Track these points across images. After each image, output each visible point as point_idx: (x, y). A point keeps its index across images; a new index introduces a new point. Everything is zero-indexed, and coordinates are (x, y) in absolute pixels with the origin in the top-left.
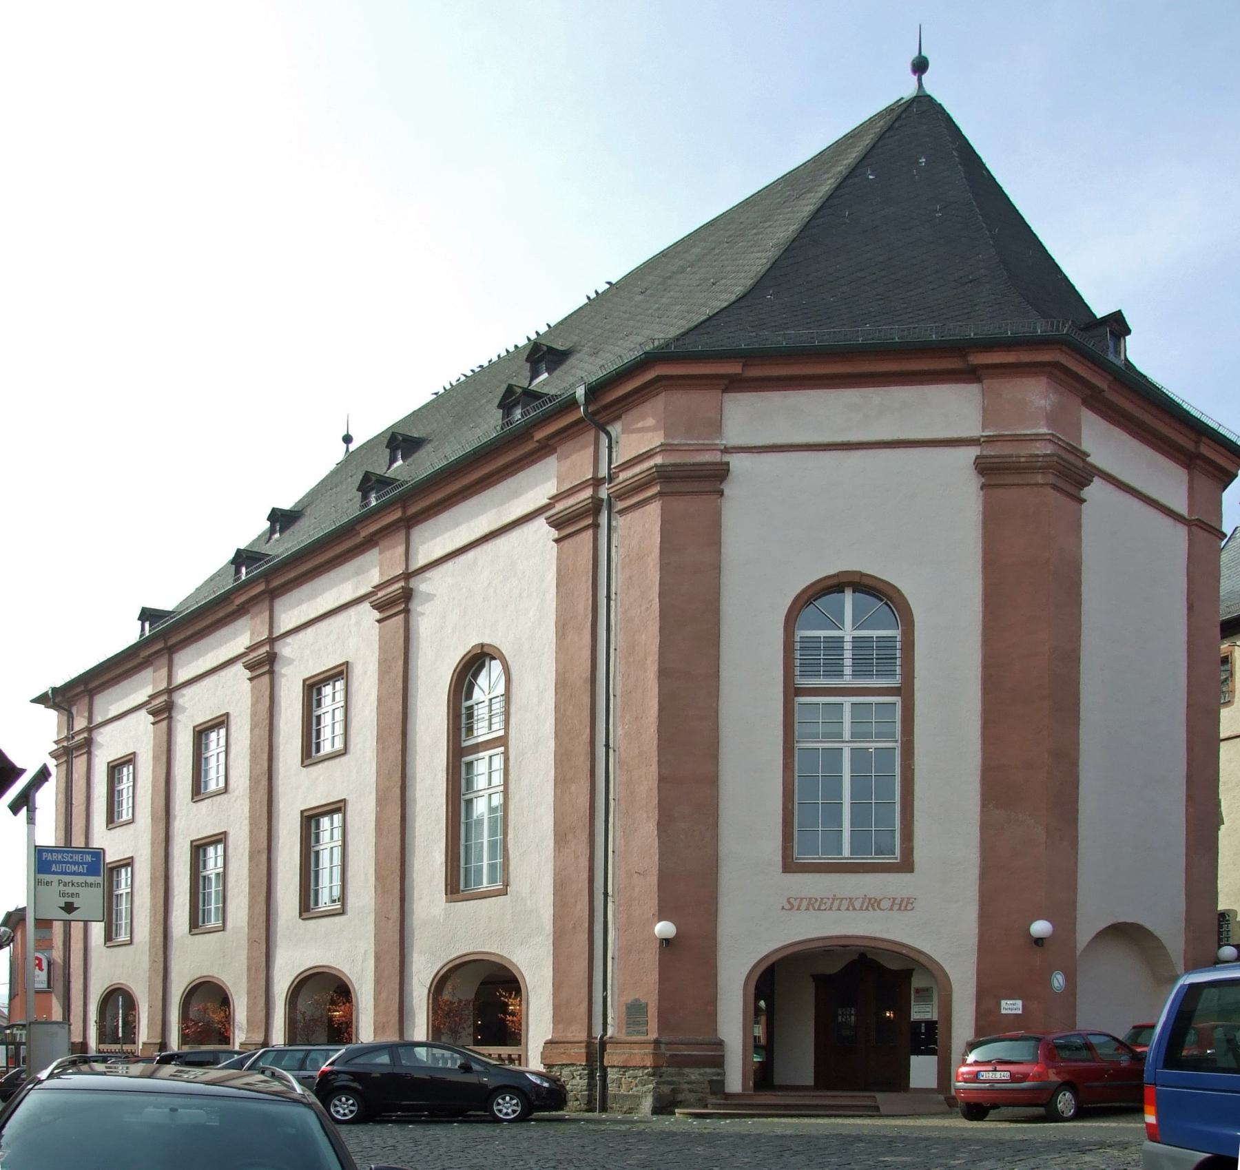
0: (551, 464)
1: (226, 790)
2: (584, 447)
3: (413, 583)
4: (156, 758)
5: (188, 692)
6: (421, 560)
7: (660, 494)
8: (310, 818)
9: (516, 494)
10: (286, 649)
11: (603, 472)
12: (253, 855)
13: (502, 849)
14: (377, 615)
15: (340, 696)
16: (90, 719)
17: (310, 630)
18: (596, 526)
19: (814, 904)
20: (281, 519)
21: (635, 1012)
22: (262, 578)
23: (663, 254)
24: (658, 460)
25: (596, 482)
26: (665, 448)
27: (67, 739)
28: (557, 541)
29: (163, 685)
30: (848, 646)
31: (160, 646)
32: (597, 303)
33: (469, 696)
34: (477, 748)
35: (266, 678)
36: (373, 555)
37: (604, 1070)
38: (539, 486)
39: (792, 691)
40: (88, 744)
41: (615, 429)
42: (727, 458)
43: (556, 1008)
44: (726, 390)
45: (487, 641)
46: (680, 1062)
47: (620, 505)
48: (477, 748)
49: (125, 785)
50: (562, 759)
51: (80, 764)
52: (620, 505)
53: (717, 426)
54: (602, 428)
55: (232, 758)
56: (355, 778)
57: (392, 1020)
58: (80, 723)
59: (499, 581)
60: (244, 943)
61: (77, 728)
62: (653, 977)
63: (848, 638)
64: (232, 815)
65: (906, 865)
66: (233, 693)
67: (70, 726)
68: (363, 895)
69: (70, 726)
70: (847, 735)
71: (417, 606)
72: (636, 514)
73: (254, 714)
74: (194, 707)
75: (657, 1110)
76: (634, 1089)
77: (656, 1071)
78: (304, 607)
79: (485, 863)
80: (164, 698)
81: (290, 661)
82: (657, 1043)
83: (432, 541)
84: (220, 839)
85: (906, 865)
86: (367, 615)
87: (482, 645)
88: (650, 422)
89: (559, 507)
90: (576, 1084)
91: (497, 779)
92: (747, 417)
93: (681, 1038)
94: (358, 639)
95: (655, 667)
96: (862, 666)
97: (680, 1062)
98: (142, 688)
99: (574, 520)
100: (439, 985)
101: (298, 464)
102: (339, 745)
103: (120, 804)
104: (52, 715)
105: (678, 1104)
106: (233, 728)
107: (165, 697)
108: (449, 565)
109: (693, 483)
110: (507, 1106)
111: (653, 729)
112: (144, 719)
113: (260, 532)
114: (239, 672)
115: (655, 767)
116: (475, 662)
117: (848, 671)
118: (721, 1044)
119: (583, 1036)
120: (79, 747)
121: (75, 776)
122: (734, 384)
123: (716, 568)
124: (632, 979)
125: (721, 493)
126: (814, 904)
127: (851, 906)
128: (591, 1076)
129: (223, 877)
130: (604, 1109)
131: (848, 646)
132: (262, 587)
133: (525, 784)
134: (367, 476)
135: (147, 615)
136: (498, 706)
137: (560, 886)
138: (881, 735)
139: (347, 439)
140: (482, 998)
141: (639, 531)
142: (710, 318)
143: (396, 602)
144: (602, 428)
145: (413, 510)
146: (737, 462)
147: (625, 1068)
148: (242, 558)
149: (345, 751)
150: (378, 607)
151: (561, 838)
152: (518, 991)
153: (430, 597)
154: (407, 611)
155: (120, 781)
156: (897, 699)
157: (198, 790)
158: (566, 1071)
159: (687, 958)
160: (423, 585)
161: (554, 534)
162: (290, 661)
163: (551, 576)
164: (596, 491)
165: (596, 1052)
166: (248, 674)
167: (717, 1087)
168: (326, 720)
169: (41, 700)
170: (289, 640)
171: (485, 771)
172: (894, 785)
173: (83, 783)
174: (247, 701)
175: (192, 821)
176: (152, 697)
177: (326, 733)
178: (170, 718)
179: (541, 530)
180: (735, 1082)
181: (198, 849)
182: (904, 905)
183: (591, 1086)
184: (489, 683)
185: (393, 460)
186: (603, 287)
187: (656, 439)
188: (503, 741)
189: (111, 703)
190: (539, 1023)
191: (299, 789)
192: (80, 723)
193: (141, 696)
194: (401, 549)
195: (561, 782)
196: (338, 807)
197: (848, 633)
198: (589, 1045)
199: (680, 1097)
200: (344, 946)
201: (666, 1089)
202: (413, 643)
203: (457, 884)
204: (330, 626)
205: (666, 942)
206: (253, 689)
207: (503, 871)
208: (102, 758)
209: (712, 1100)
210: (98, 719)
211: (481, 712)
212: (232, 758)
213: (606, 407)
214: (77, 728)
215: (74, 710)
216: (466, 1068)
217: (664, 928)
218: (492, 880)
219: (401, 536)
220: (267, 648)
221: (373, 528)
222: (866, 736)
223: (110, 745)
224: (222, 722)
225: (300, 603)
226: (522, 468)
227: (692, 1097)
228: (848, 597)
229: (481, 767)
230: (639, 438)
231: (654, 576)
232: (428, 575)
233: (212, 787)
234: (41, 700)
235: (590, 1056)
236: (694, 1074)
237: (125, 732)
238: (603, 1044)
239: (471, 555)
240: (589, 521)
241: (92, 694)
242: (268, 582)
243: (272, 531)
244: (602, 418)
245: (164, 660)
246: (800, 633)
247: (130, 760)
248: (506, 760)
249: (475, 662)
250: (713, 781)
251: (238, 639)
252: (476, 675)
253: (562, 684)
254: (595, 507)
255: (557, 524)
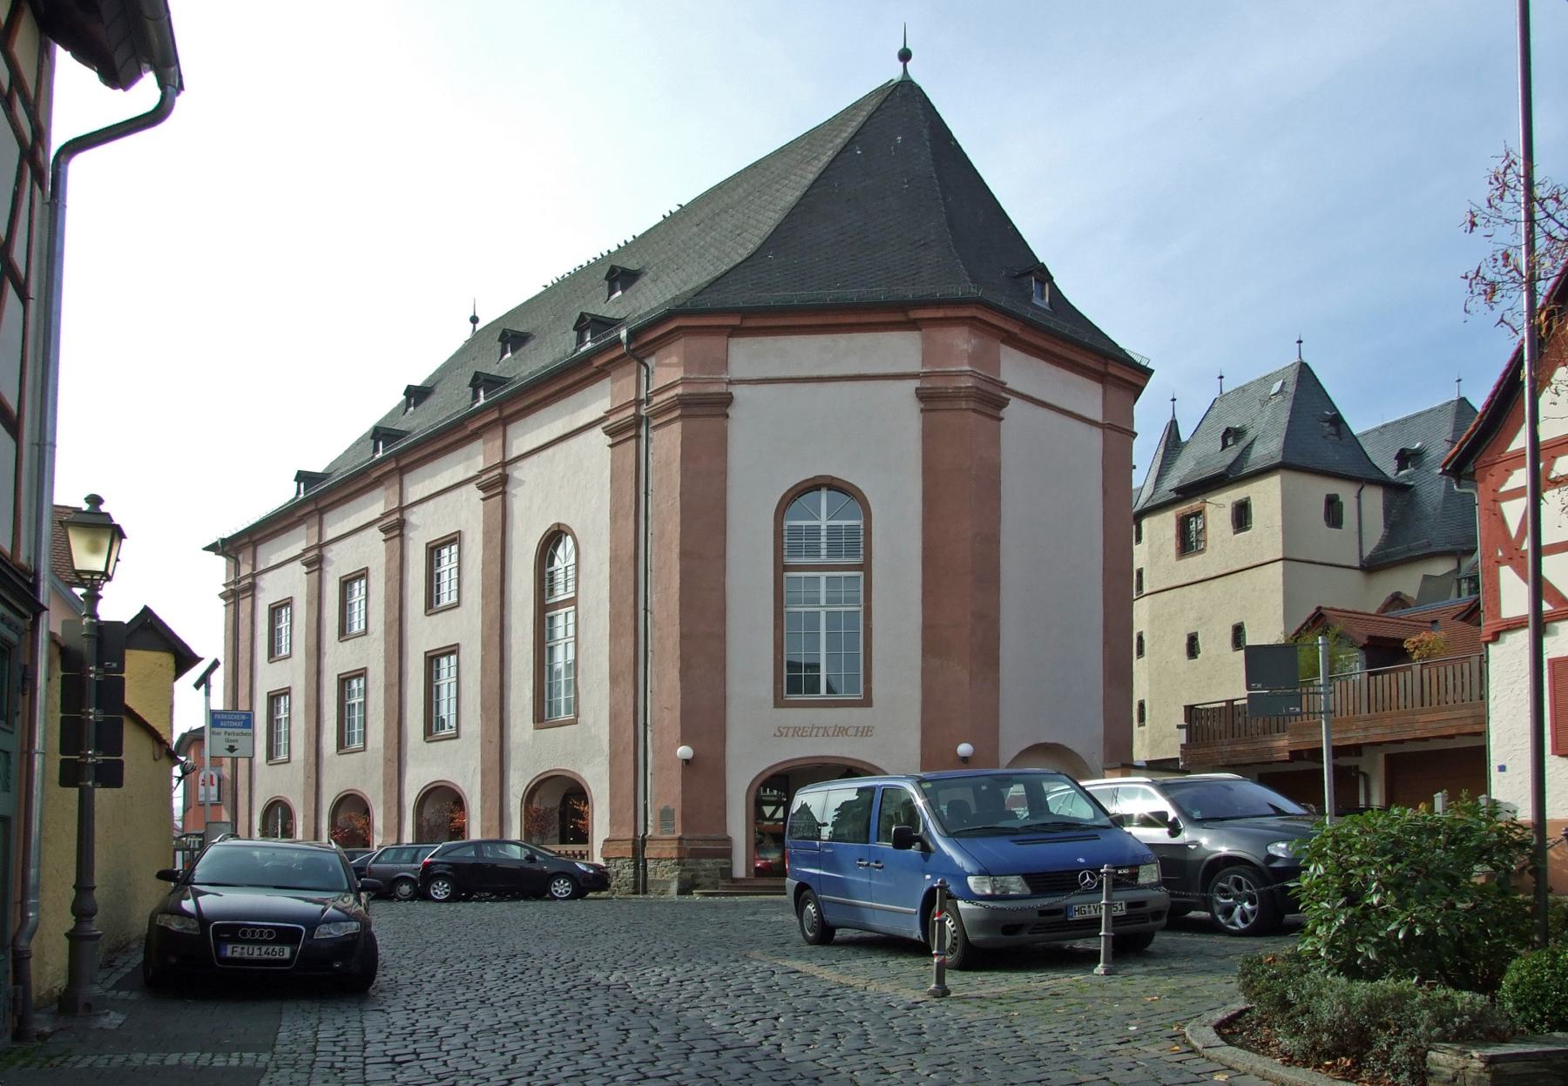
0: (605, 385)
1: (366, 632)
2: (630, 374)
3: (509, 470)
4: (309, 603)
5: (335, 547)
6: (515, 451)
7: (681, 417)
8: (432, 658)
9: (583, 406)
10: (414, 517)
11: (643, 396)
12: (387, 688)
13: (574, 686)
14: (481, 494)
15: (454, 558)
16: (254, 568)
17: (431, 503)
18: (638, 437)
19: (798, 732)
20: (416, 395)
21: (666, 815)
22: (394, 453)
23: (720, 186)
24: (679, 390)
25: (638, 403)
26: (684, 381)
27: (234, 582)
28: (611, 446)
29: (315, 541)
30: (823, 533)
31: (312, 507)
32: (671, 221)
33: (551, 564)
34: (556, 606)
35: (397, 541)
36: (478, 445)
37: (645, 860)
38: (597, 402)
39: (781, 568)
40: (253, 588)
41: (651, 362)
42: (732, 389)
43: (612, 813)
44: (730, 336)
45: (562, 521)
46: (698, 854)
47: (655, 422)
48: (556, 606)
49: (284, 625)
50: (615, 617)
51: (245, 605)
52: (655, 422)
53: (725, 364)
54: (641, 361)
55: (371, 605)
56: (464, 626)
57: (496, 826)
58: (246, 570)
59: (569, 472)
60: (381, 761)
61: (243, 574)
62: (678, 789)
63: (824, 527)
64: (370, 653)
65: (867, 702)
66: (371, 550)
67: (237, 572)
68: (472, 723)
69: (237, 572)
70: (823, 602)
71: (513, 490)
72: (664, 430)
73: (387, 570)
74: (340, 562)
75: (681, 892)
76: (665, 875)
77: (680, 861)
78: (427, 482)
79: (563, 698)
80: (316, 552)
81: (416, 527)
82: (680, 839)
83: (525, 437)
84: (361, 673)
85: (867, 702)
86: (473, 494)
87: (559, 525)
88: (674, 360)
89: (612, 420)
90: (624, 872)
91: (571, 632)
92: (748, 356)
93: (698, 835)
94: (466, 512)
95: (677, 550)
96: (833, 550)
97: (698, 854)
98: (297, 542)
99: (626, 430)
100: (530, 795)
101: (429, 344)
102: (454, 599)
103: (280, 641)
104: (221, 561)
105: (697, 886)
106: (371, 580)
107: (316, 552)
108: (535, 458)
109: (706, 408)
110: (561, 888)
111: (677, 597)
112: (298, 569)
113: (395, 405)
114: (375, 534)
115: (677, 627)
116: (554, 537)
117: (824, 552)
118: (728, 840)
119: (631, 835)
120: (244, 590)
121: (242, 615)
122: (736, 332)
123: (723, 473)
124: (665, 791)
125: (727, 416)
126: (798, 732)
127: (826, 733)
128: (636, 866)
129: (364, 704)
130: (645, 892)
131: (823, 533)
132: (393, 465)
133: (588, 640)
134: (477, 376)
135: (302, 477)
136: (571, 573)
137: (614, 717)
138: (848, 601)
139: (474, 320)
140: (561, 804)
141: (667, 442)
142: (727, 272)
143: (496, 485)
144: (641, 361)
145: (507, 412)
146: (737, 391)
147: (659, 859)
148: (381, 434)
149: (458, 605)
150: (482, 488)
151: (614, 679)
152: (586, 803)
153: (521, 483)
154: (504, 493)
155: (280, 621)
156: (861, 574)
157: (344, 631)
158: (619, 863)
159: (703, 774)
160: (517, 472)
161: (609, 440)
162: (416, 527)
163: (607, 473)
164: (638, 410)
165: (639, 846)
166: (383, 536)
167: (727, 873)
168: (445, 577)
169: (212, 548)
170: (415, 509)
171: (562, 622)
172: (858, 635)
173: (248, 621)
174: (383, 559)
175: (339, 658)
176: (306, 551)
177: (445, 588)
178: (320, 569)
179: (598, 438)
180: (740, 870)
181: (344, 681)
182: (866, 732)
183: (636, 874)
184: (564, 555)
185: (504, 353)
186: (675, 209)
187: (677, 374)
188: (573, 601)
189: (272, 553)
190: (600, 826)
191: (424, 634)
192: (246, 570)
193: (297, 549)
194: (499, 442)
195: (614, 636)
196: (453, 650)
197: (824, 523)
198: (635, 841)
199: (698, 881)
200: (457, 763)
201: (688, 875)
202: (509, 520)
203: (542, 717)
204: (445, 499)
205: (687, 762)
206: (387, 549)
207: (574, 707)
208: (264, 602)
209: (723, 883)
210: (261, 567)
211: (560, 576)
212: (371, 605)
213: (643, 346)
214: (243, 574)
215: (240, 558)
216: (531, 859)
217: (684, 751)
218: (568, 712)
219: (499, 431)
220: (398, 515)
221: (478, 424)
222: (837, 601)
223: (271, 590)
224: (363, 574)
225: (424, 478)
226: (587, 386)
227: (708, 881)
228: (824, 495)
229: (560, 621)
230: (668, 371)
231: (677, 479)
232: (519, 464)
233: (356, 629)
234: (212, 548)
235: (635, 851)
236: (708, 863)
237: (283, 580)
238: (644, 841)
239: (550, 451)
240: (632, 433)
241: (255, 545)
242: (397, 461)
243: (407, 404)
244: (639, 354)
245: (316, 519)
246: (788, 523)
247: (288, 603)
248: (576, 617)
249: (554, 537)
250: (722, 637)
251: (375, 506)
252: (556, 548)
253: (614, 560)
254: (637, 422)
255: (610, 432)
